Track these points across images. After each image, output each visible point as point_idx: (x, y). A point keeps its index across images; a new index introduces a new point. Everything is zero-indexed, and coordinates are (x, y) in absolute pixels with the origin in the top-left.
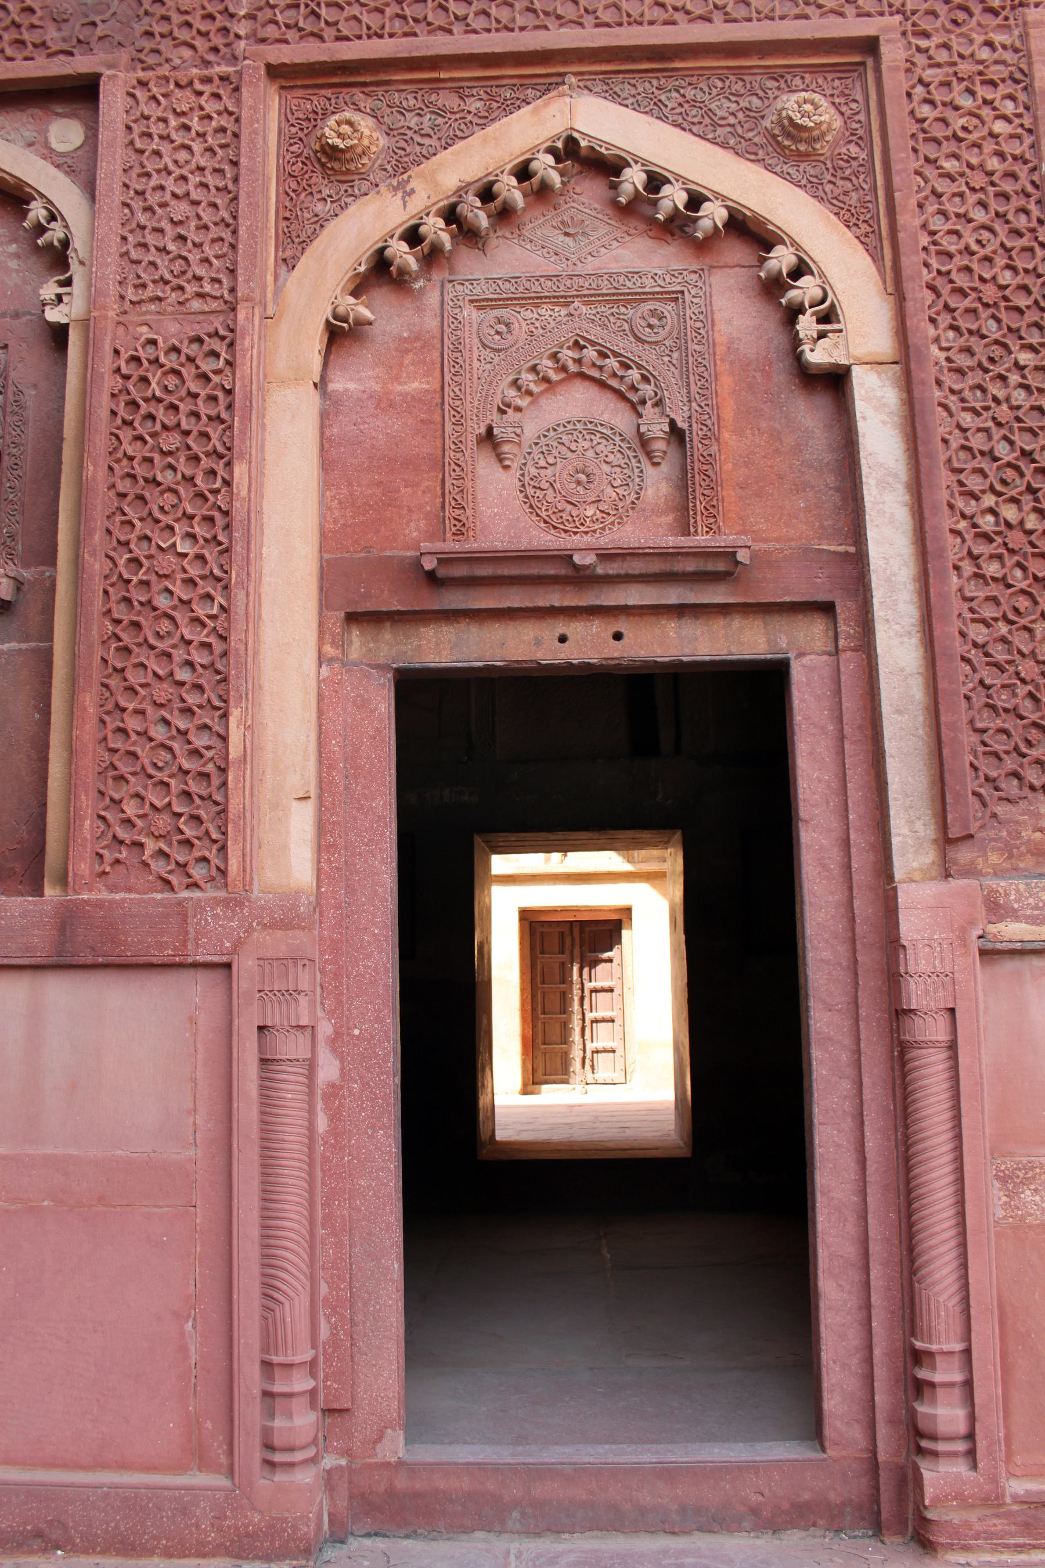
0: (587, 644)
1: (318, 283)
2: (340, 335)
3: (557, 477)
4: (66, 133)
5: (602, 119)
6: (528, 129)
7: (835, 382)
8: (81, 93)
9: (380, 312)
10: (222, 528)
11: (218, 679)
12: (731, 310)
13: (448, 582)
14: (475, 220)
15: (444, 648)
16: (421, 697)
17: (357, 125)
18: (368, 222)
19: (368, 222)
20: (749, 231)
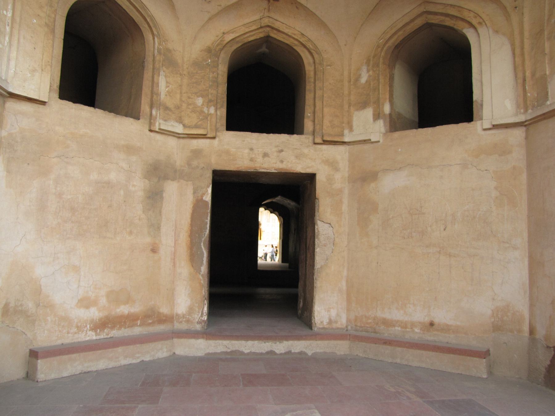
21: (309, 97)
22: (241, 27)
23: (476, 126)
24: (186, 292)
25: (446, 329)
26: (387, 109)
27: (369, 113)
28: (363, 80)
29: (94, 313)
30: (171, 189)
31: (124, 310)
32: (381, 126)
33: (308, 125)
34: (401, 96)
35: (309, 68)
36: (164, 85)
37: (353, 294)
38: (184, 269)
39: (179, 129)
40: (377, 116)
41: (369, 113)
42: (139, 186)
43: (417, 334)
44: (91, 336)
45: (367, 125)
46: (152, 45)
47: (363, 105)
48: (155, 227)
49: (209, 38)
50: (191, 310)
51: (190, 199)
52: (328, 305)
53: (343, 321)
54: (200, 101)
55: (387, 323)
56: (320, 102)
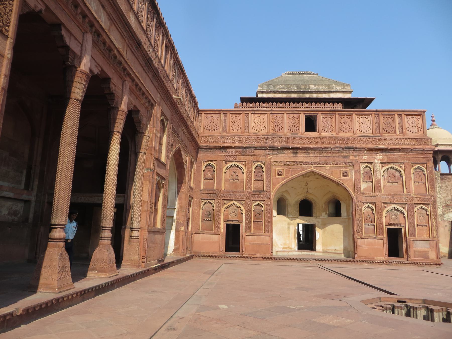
0: (233, 223)
1: (223, 209)
2: (224, 211)
3: (233, 217)
4: (214, 201)
5: (235, 202)
6: (232, 202)
7: (243, 214)
8: (214, 200)
9: (226, 210)
10: (220, 218)
11: (220, 224)
12: (239, 211)
13: (228, 221)
14: (230, 206)
15: (228, 223)
16: (226, 224)
17: (225, 202)
18: (225, 206)
19: (225, 206)
20: (240, 207)
21: (314, 210)
22: (301, 197)
23: (341, 218)
24: (294, 245)
25: (337, 250)
26: (328, 213)
27: (324, 213)
28: (324, 207)
29: (282, 247)
30: (291, 226)
31: (285, 246)
32: (327, 216)
33: (314, 215)
34: (331, 209)
35: (314, 204)
36: (289, 209)
37: (323, 245)
38: (293, 240)
39: (292, 216)
40: (326, 214)
41: (324, 213)
42: (287, 226)
43: (333, 251)
44: (282, 250)
45: (324, 215)
46: (287, 203)
47: (324, 212)
48: (289, 233)
49: (296, 200)
50: (295, 247)
51: (294, 228)
52: (319, 246)
53: (321, 250)
54: (295, 211)
55: (328, 250)
56: (316, 211)
